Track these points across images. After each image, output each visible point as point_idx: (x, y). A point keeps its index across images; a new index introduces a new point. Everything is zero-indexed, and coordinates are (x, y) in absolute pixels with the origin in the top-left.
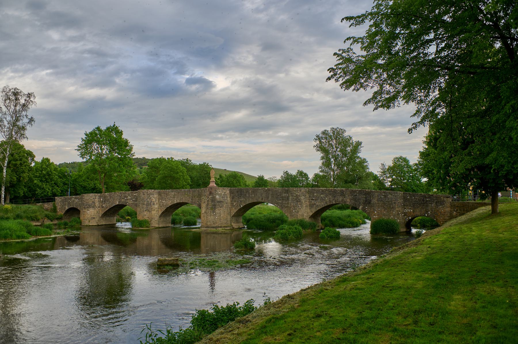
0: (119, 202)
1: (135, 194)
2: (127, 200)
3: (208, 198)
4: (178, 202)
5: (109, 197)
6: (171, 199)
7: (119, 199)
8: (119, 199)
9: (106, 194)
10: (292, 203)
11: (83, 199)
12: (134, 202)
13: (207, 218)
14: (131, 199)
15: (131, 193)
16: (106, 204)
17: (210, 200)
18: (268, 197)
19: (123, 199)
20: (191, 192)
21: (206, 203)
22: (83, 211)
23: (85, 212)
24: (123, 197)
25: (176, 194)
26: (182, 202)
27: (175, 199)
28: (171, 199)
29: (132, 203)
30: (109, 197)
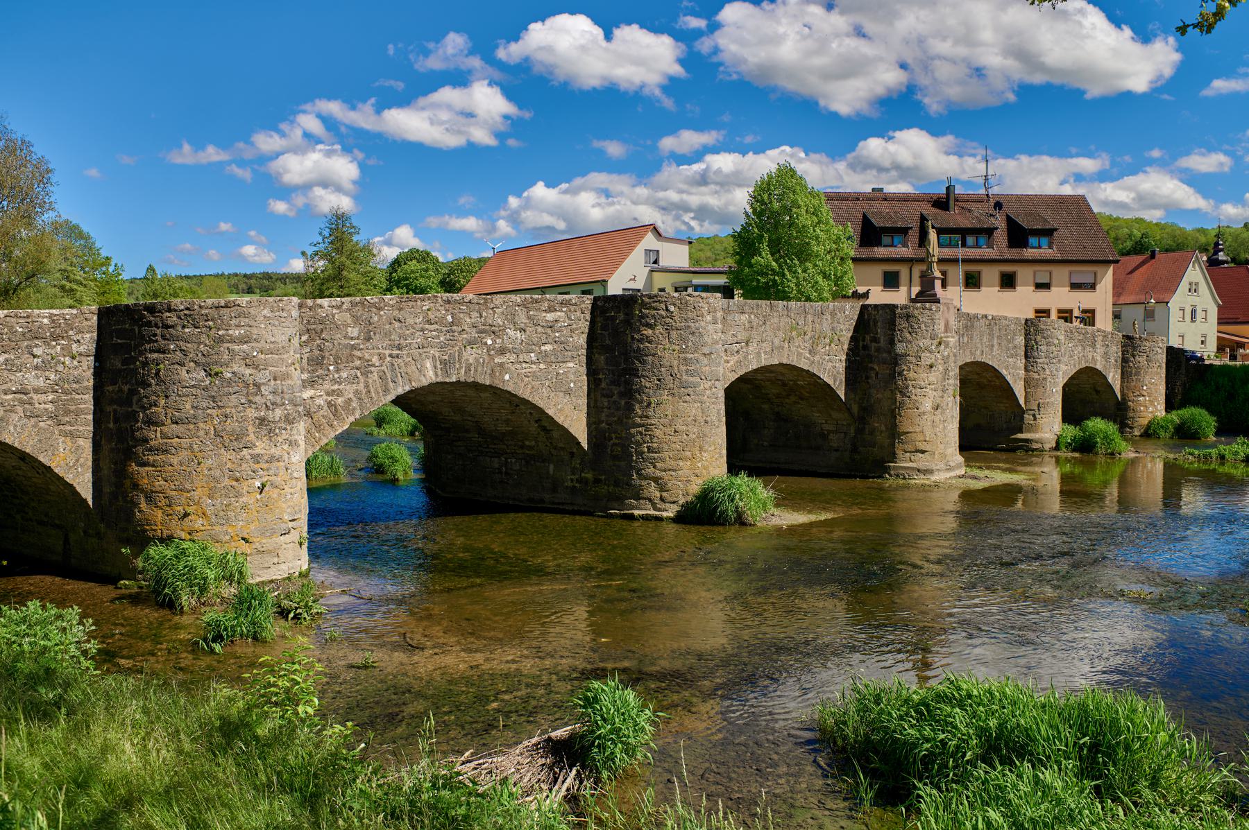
0: (446, 365)
1: (550, 316)
2: (502, 351)
3: (947, 346)
4: (764, 363)
5: (353, 331)
6: (735, 347)
7: (442, 347)
8: (442, 347)
9: (325, 302)
10: (1046, 366)
11: (244, 340)
12: (549, 364)
13: (945, 428)
14: (530, 346)
15: (523, 304)
16: (327, 385)
17: (951, 355)
18: (993, 346)
19: (471, 343)
20: (810, 317)
21: (941, 368)
22: (256, 458)
23: (272, 459)
24: (474, 334)
25: (755, 321)
26: (776, 362)
27: (752, 347)
28: (735, 347)
29: (535, 376)
30: (353, 331)
